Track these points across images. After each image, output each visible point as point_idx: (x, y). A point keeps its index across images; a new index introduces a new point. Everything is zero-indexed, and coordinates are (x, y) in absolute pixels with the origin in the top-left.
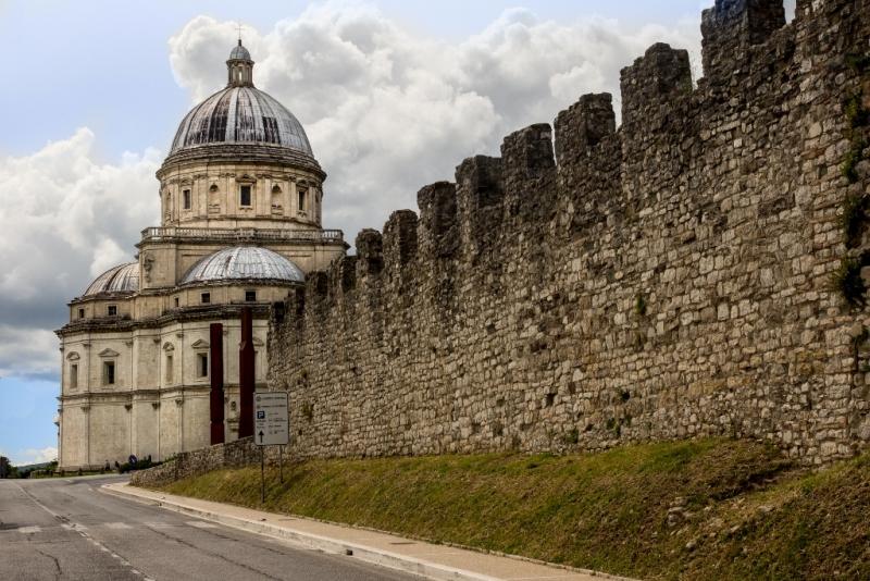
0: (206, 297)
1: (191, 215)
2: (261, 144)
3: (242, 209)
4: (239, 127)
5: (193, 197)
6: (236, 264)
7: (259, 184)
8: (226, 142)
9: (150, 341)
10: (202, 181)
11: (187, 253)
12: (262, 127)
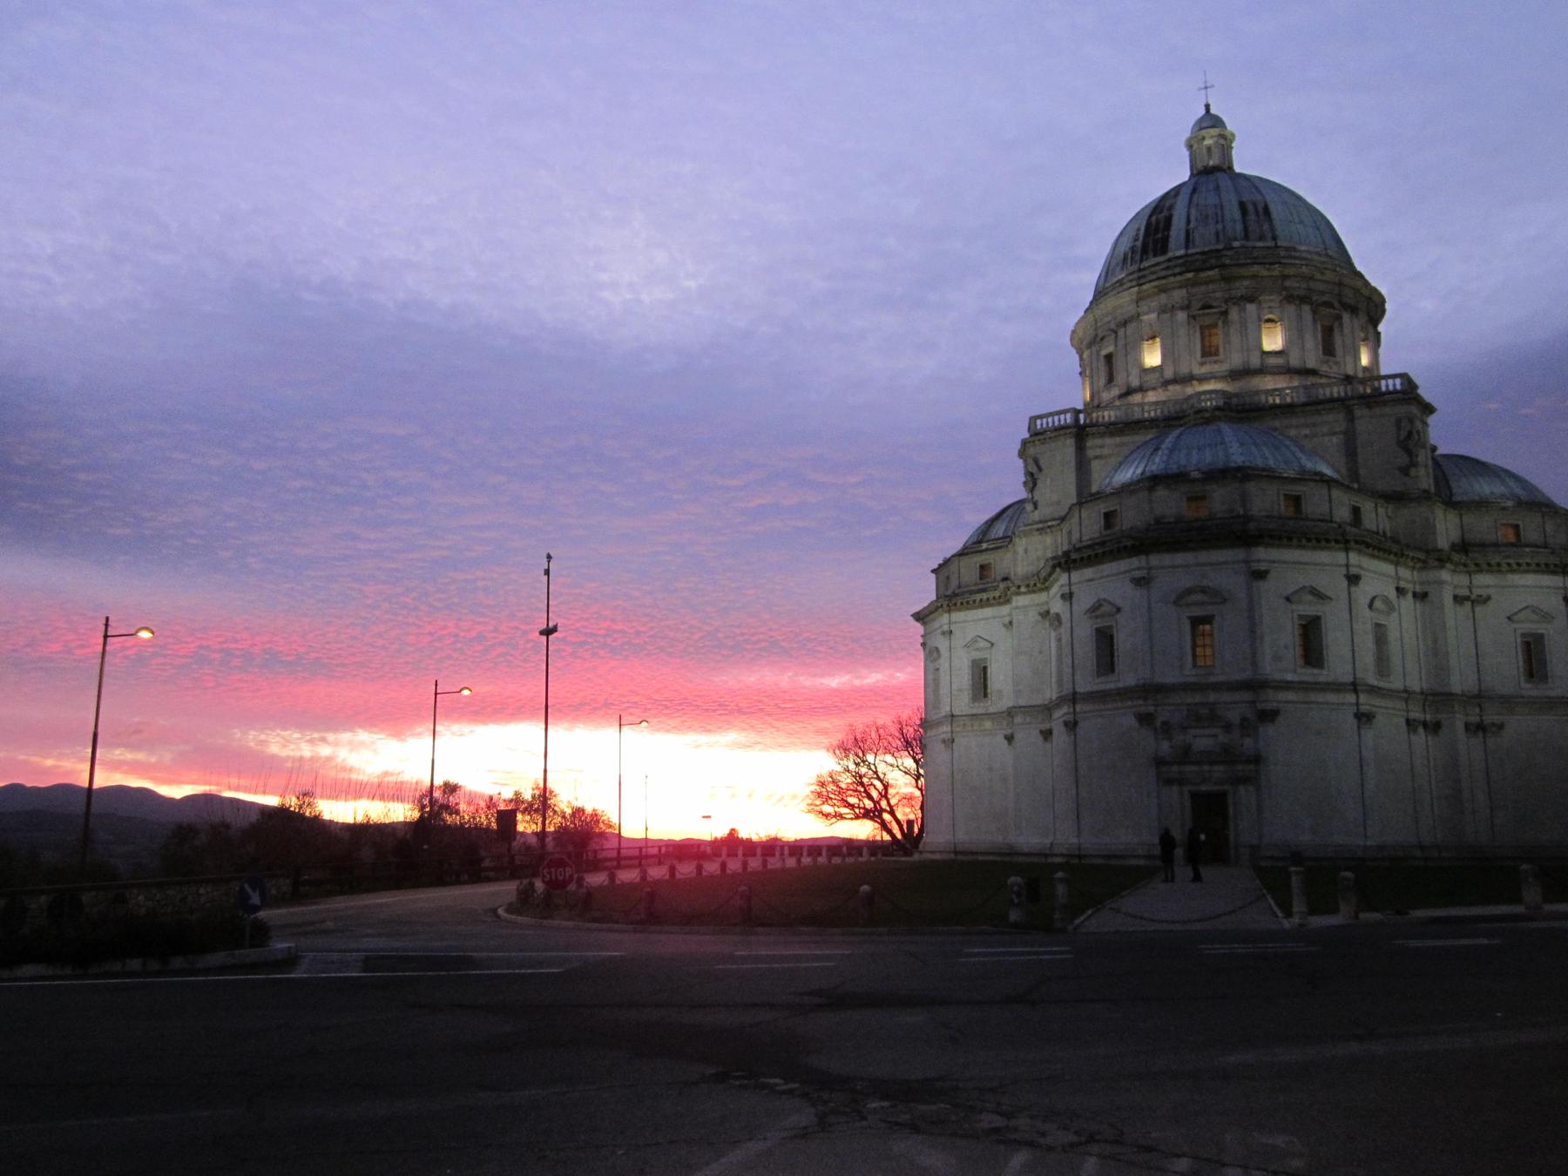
0: (1109, 517)
1: (1115, 392)
2: (1236, 244)
3: (1202, 364)
4: (1192, 225)
5: (1118, 362)
6: (1172, 451)
7: (1234, 314)
8: (1170, 254)
9: (1033, 615)
10: (1131, 328)
11: (1098, 452)
12: (1237, 214)
